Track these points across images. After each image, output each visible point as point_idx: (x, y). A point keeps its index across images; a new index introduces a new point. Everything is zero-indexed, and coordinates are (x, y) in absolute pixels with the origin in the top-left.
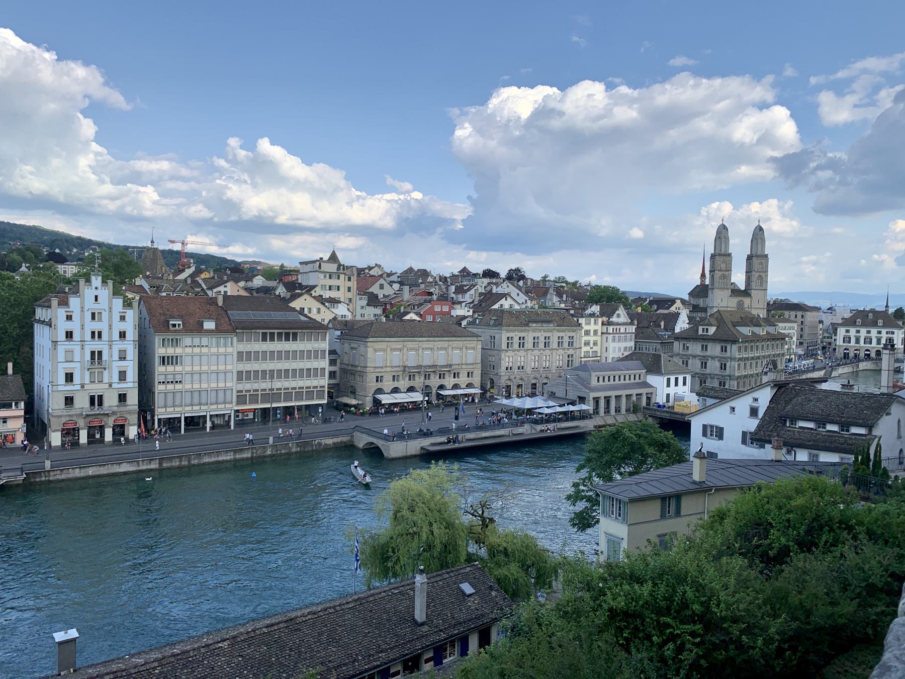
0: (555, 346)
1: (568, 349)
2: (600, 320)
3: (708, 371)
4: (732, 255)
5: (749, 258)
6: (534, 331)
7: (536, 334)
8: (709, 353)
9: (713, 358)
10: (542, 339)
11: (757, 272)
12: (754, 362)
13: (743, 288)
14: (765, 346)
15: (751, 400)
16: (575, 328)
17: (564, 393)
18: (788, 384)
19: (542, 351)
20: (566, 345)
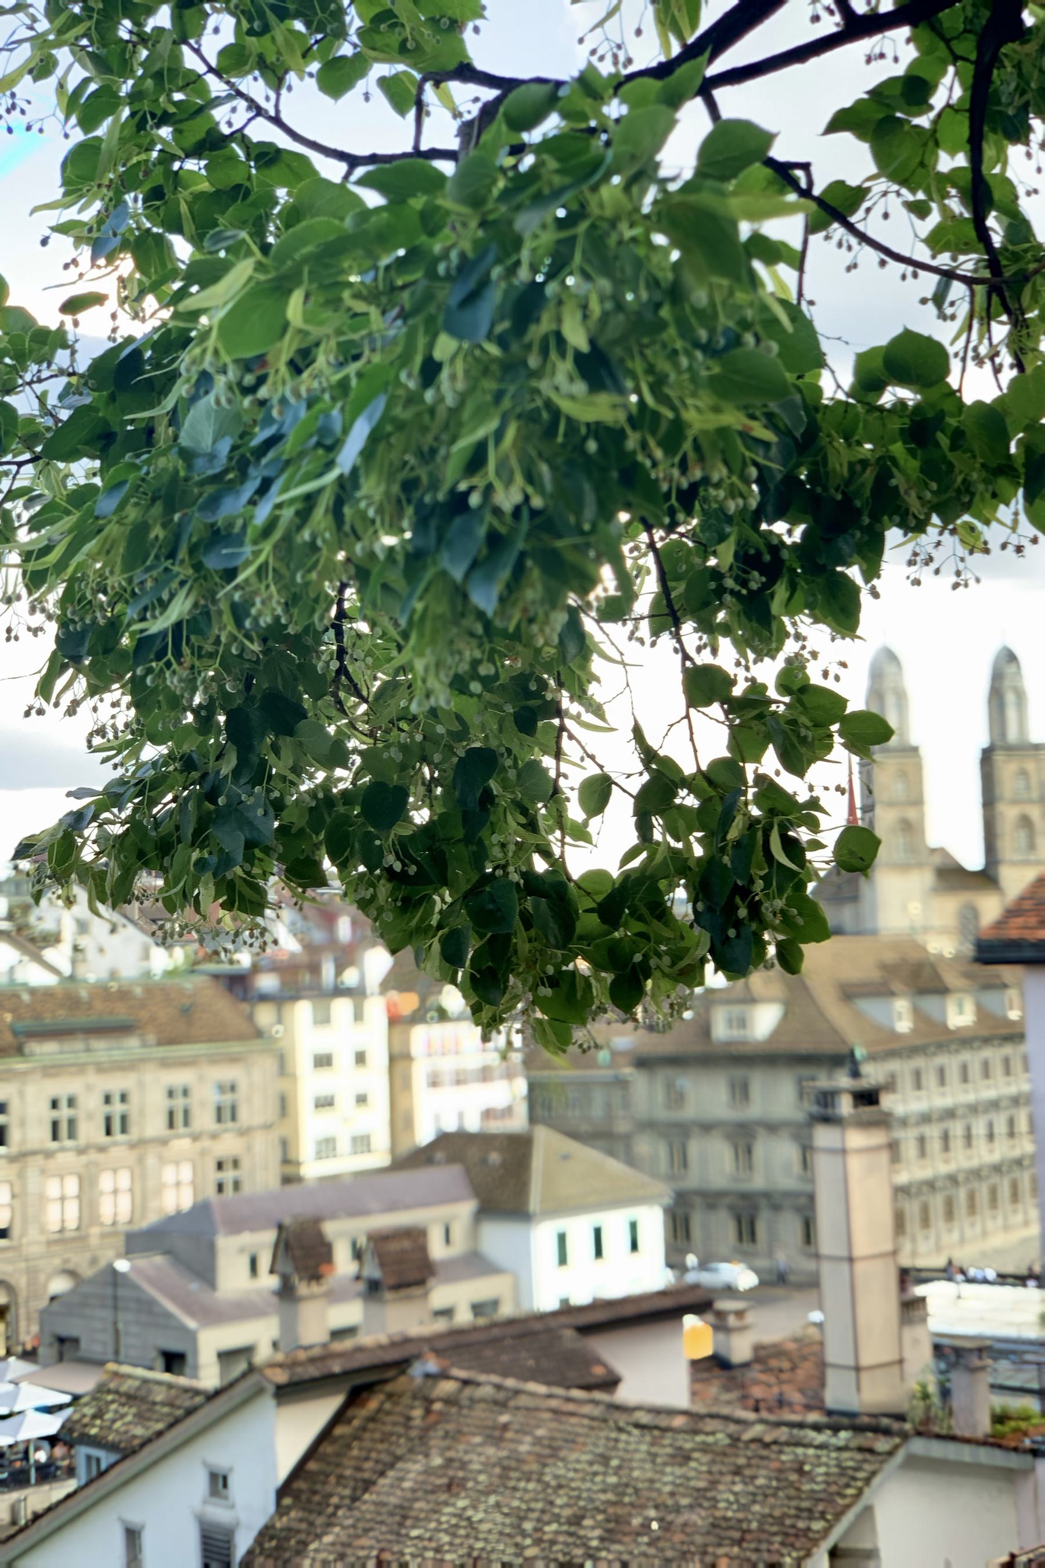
0: (154, 1125)
1: (214, 1136)
2: (376, 1008)
3: (758, 1182)
4: (923, 752)
5: (987, 757)
6: (51, 1070)
7: (62, 1087)
8: (755, 1110)
9: (773, 1128)
10: (91, 1104)
11: (1015, 802)
12: (933, 1132)
13: (973, 860)
14: (975, 1071)
15: (200, 1483)
16: (236, 1048)
17: (108, 1337)
18: (402, 1365)
19: (93, 1156)
20: (204, 1119)
